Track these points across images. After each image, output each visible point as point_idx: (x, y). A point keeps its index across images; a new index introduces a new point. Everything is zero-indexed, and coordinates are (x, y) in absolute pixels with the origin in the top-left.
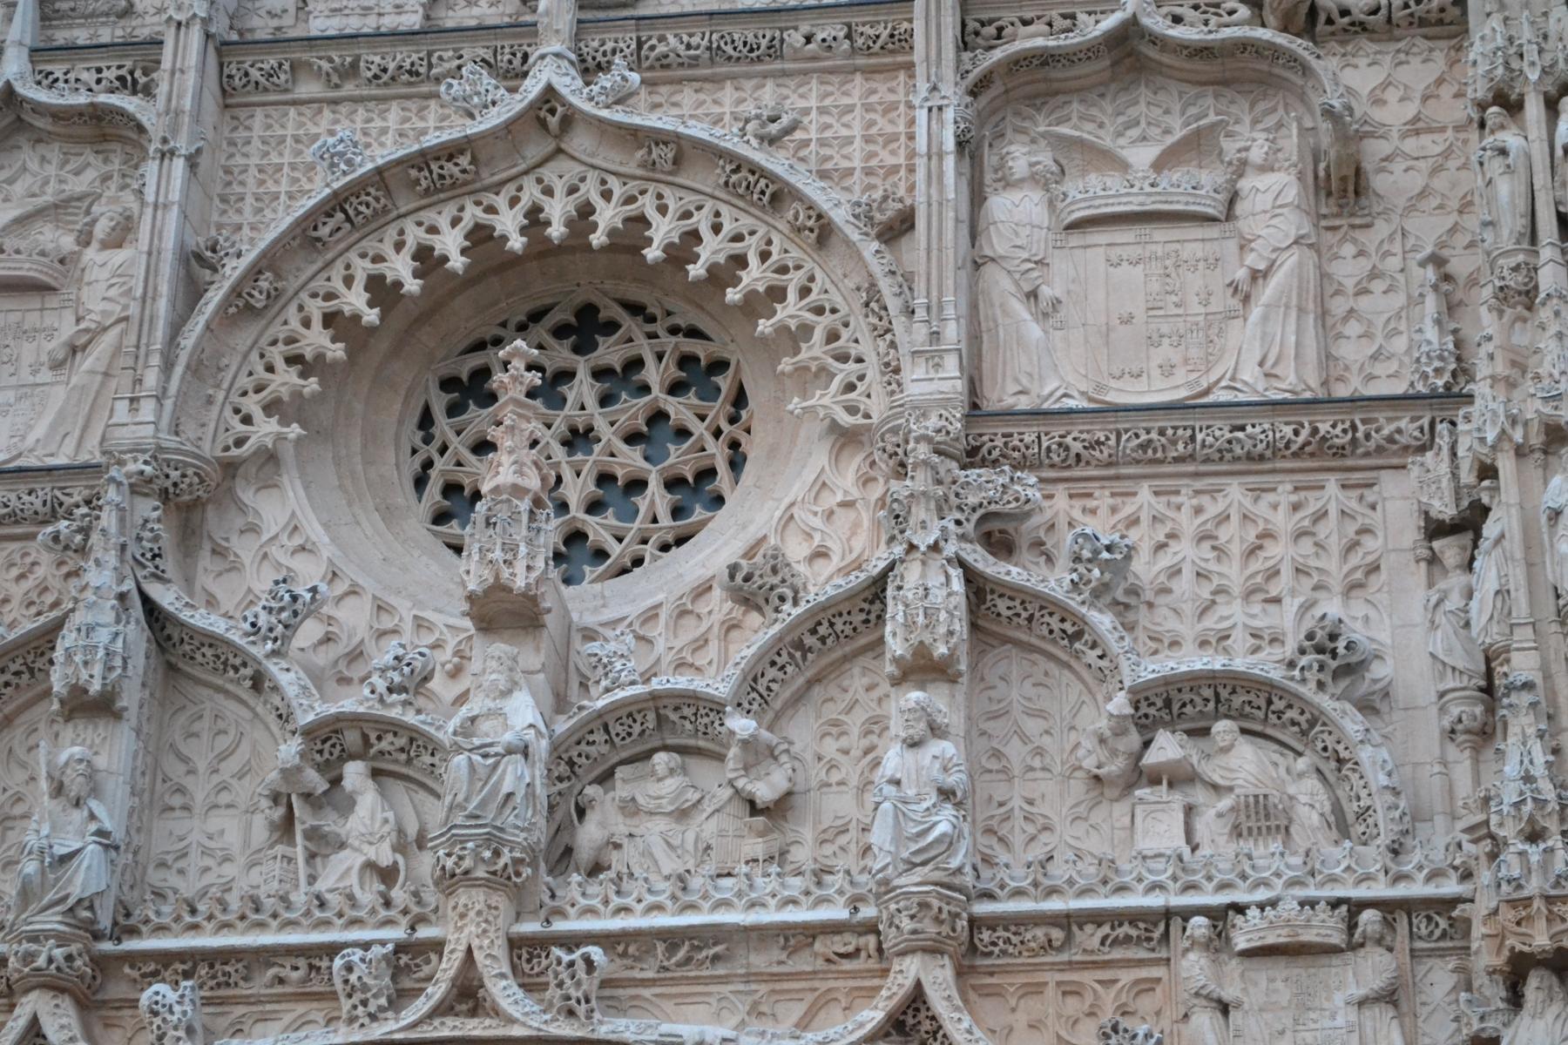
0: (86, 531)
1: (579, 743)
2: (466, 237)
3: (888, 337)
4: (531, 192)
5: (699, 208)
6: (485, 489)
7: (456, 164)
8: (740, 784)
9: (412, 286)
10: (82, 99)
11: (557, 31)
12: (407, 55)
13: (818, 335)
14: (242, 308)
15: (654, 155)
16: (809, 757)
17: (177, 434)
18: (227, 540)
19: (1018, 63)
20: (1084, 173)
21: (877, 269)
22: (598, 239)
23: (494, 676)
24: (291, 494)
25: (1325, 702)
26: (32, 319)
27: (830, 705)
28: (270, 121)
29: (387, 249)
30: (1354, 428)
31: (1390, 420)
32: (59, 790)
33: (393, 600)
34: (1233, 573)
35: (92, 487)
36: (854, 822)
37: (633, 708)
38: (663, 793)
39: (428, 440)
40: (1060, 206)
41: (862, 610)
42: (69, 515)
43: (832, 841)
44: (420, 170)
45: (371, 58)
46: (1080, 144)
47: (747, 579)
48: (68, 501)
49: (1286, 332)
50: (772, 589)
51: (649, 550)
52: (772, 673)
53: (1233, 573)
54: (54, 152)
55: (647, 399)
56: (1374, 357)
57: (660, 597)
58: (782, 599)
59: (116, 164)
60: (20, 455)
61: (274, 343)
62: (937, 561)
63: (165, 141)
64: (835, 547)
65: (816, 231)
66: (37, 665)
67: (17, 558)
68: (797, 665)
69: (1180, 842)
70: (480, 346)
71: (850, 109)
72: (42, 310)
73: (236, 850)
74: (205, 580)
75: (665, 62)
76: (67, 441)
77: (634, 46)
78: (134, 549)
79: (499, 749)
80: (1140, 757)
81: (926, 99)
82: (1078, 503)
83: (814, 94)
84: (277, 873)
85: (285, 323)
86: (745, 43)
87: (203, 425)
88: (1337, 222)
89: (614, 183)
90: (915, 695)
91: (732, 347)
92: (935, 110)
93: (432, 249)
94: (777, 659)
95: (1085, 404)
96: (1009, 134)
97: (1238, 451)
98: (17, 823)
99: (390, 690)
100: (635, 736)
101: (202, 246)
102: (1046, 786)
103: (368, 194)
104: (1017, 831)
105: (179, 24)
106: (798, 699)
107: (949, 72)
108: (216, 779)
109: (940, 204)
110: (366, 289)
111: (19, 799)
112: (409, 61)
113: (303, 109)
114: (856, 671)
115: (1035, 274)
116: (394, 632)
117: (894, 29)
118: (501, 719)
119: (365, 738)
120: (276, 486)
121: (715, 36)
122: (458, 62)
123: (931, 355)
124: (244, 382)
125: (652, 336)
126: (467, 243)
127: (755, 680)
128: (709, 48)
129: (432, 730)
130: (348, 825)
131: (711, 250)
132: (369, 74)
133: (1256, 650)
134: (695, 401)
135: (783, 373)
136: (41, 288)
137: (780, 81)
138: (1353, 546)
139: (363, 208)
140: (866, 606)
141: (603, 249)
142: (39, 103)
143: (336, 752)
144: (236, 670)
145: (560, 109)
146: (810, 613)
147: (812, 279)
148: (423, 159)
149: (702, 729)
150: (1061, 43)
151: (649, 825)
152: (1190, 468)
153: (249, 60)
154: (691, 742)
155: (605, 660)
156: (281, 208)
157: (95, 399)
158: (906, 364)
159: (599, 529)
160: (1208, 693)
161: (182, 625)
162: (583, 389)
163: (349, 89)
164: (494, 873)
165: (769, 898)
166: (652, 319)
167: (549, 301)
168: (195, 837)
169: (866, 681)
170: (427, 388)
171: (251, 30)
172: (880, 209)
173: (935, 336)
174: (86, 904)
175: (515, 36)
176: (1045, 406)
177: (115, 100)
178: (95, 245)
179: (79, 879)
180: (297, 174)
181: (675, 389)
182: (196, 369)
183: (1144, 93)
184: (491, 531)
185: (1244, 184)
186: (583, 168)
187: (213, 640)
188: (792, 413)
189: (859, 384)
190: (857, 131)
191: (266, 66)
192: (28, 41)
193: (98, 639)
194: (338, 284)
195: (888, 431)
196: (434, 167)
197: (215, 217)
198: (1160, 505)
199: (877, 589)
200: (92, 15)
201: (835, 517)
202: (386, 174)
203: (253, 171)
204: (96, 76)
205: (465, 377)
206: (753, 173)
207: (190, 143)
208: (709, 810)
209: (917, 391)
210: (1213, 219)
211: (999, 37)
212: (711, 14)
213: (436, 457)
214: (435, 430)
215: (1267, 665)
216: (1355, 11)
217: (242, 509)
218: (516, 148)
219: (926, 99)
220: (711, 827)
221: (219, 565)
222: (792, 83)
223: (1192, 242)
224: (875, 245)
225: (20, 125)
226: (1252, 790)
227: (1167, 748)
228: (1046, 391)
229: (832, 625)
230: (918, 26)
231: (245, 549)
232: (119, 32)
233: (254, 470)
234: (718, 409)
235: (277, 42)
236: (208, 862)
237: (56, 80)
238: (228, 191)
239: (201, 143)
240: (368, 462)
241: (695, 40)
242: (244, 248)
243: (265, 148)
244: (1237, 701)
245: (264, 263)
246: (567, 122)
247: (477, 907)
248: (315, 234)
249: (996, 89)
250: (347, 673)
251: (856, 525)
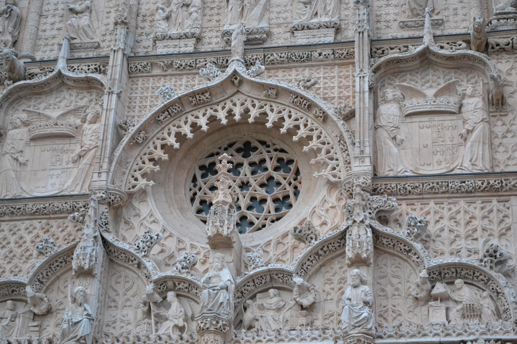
0: (83, 216)
1: (244, 286)
2: (208, 120)
3: (347, 152)
4: (229, 105)
5: (284, 110)
6: (214, 202)
7: (205, 96)
8: (298, 299)
9: (190, 135)
10: (83, 75)
11: (238, 52)
12: (188, 60)
13: (323, 152)
14: (135, 143)
15: (269, 93)
16: (320, 291)
17: (113, 184)
18: (129, 219)
19: (389, 62)
20: (411, 98)
21: (343, 130)
22: (251, 120)
23: (217, 264)
24: (150, 204)
25: (493, 273)
26: (67, 147)
27: (327, 274)
28: (144, 82)
29: (182, 123)
30: (502, 182)
31: (514, 179)
32: (74, 301)
33: (183, 239)
34: (462, 230)
35: (86, 201)
36: (336, 313)
37: (262, 274)
38: (272, 302)
39: (195, 186)
40: (403, 109)
41: (338, 242)
42: (78, 210)
43: (328, 319)
44: (193, 98)
45: (177, 61)
46: (410, 89)
47: (300, 232)
48: (78, 206)
49: (479, 151)
50: (308, 235)
51: (268, 222)
52: (308, 263)
53: (462, 230)
54: (74, 92)
55: (267, 172)
56: (508, 159)
57: (271, 238)
58: (312, 238)
59: (94, 96)
60: (62, 191)
61: (145, 154)
62: (363, 226)
63: (110, 89)
64: (329, 221)
65: (323, 117)
66: (67, 260)
67: (61, 224)
68: (317, 261)
69: (444, 320)
70: (212, 155)
71: (334, 77)
72: (70, 144)
73: (132, 320)
74: (122, 232)
75: (273, 62)
76: (78, 186)
77: (263, 57)
78: (99, 222)
79: (218, 288)
80: (431, 291)
81: (359, 74)
82: (410, 207)
83: (322, 73)
84: (145, 328)
85: (149, 148)
86: (299, 56)
87: (122, 181)
88: (496, 114)
89: (256, 102)
90: (356, 271)
91: (295, 155)
92: (362, 77)
93: (197, 124)
94: (310, 258)
95: (412, 174)
96: (386, 85)
97: (463, 190)
98: (60, 311)
99: (183, 268)
100: (263, 284)
101: (122, 123)
102: (399, 301)
103: (176, 106)
104: (390, 316)
105: (115, 51)
106: (317, 271)
107: (366, 65)
108: (125, 297)
109: (364, 108)
110: (175, 137)
111: (62, 304)
112: (189, 62)
113: (155, 78)
114: (336, 262)
115: (395, 131)
116: (184, 249)
117: (348, 51)
118: (219, 278)
119: (174, 284)
120: (145, 201)
121: (289, 54)
122: (205, 63)
123: (361, 158)
124: (135, 167)
125: (269, 152)
126: (208, 122)
127: (303, 265)
128: (287, 58)
129: (196, 281)
130: (169, 313)
131: (288, 124)
132: (176, 67)
133: (469, 256)
134: (283, 173)
135: (312, 164)
137: (310, 68)
138: (502, 221)
139: (174, 110)
140: (339, 241)
141: (252, 123)
142: (69, 77)
143: (165, 288)
144: (132, 261)
145: (238, 78)
146: (321, 243)
147: (321, 133)
148: (193, 94)
149: (285, 281)
150: (403, 55)
151: (268, 313)
152: (447, 195)
153: (137, 62)
154: (282, 286)
155: (253, 258)
156: (147, 110)
157: (87, 173)
158: (352, 161)
159: (251, 215)
160: (453, 270)
161: (115, 246)
162: (246, 169)
163: (170, 71)
164: (217, 329)
165: (307, 338)
166: (268, 146)
167: (234, 140)
168: (119, 316)
169: (339, 266)
170: (195, 169)
171: (138, 53)
172: (344, 110)
173: (362, 152)
174: (83, 338)
175: (224, 54)
176: (399, 175)
177: (94, 75)
178: (87, 122)
179: (81, 330)
180: (153, 99)
181: (276, 169)
182: (120, 163)
183: (431, 71)
184: (216, 216)
185: (465, 102)
186: (246, 97)
187: (125, 252)
188: (315, 177)
189: (337, 168)
190: (336, 84)
191: (143, 64)
192: (66, 57)
193: (88, 252)
194: (166, 135)
195: (347, 183)
196: (197, 97)
197: (126, 113)
198: (437, 207)
199: (343, 236)
200: (86, 48)
201: (329, 211)
202: (182, 99)
203: (138, 98)
204: (88, 68)
205: (207, 165)
206: (302, 98)
207: (118, 89)
208: (288, 308)
209: (356, 170)
210: (454, 113)
211: (383, 53)
212: (288, 47)
213: (198, 191)
214: (197, 183)
215: (473, 261)
216: (501, 44)
217: (134, 208)
218: (224, 91)
219: (359, 74)
220: (288, 315)
221: (127, 227)
222: (314, 69)
223: (447, 121)
224: (342, 122)
225: (63, 84)
226: (468, 303)
227: (440, 288)
228: (399, 170)
229: (328, 247)
230: (356, 50)
231: (136, 222)
232: (95, 54)
233: (138, 196)
234: (290, 176)
235: (146, 57)
236: (123, 324)
237: (75, 69)
238: (130, 105)
239: (122, 89)
240: (175, 193)
241: (283, 55)
242: (135, 123)
243: (142, 91)
244: (463, 273)
245: (142, 128)
246: (241, 82)
247: (211, 340)
248: (159, 119)
249: (382, 71)
250: (169, 263)
251: (336, 214)
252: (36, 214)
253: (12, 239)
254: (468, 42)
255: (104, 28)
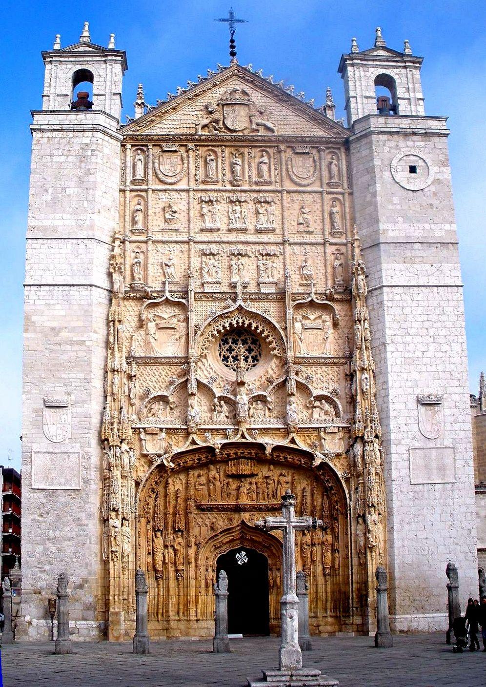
10: (177, 300)
22: (246, 326)
136: (174, 328)
187: (204, 384)
252: (167, 364)
253: (157, 373)
254: (326, 296)
255: (180, 274)
